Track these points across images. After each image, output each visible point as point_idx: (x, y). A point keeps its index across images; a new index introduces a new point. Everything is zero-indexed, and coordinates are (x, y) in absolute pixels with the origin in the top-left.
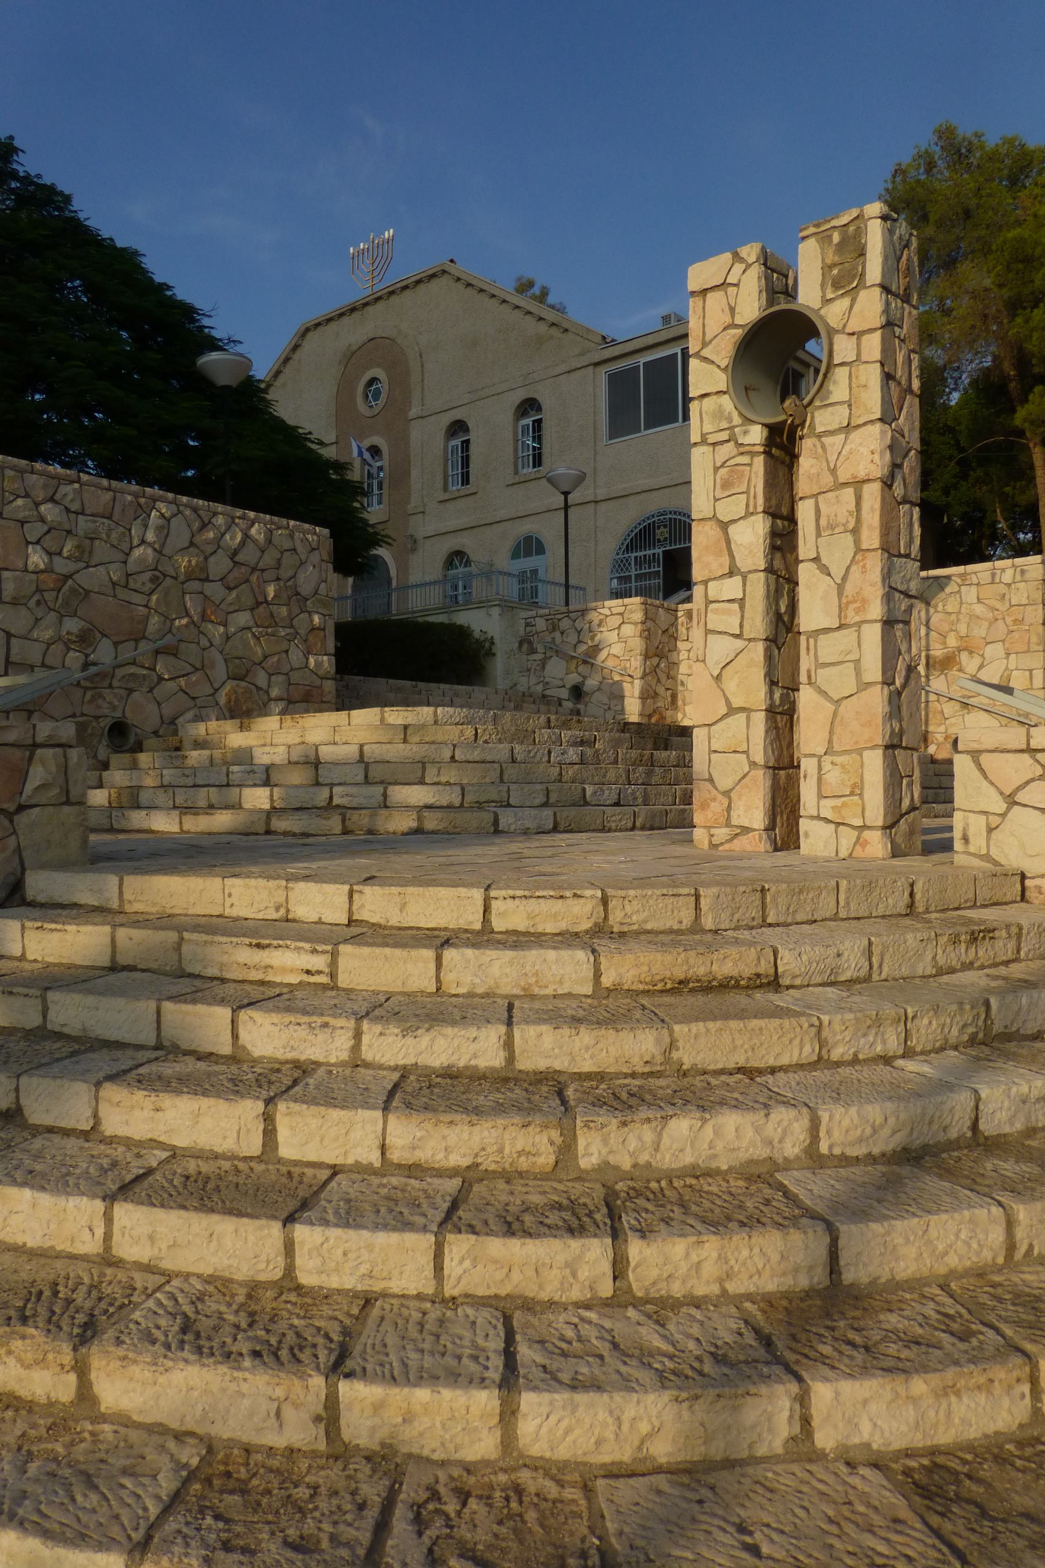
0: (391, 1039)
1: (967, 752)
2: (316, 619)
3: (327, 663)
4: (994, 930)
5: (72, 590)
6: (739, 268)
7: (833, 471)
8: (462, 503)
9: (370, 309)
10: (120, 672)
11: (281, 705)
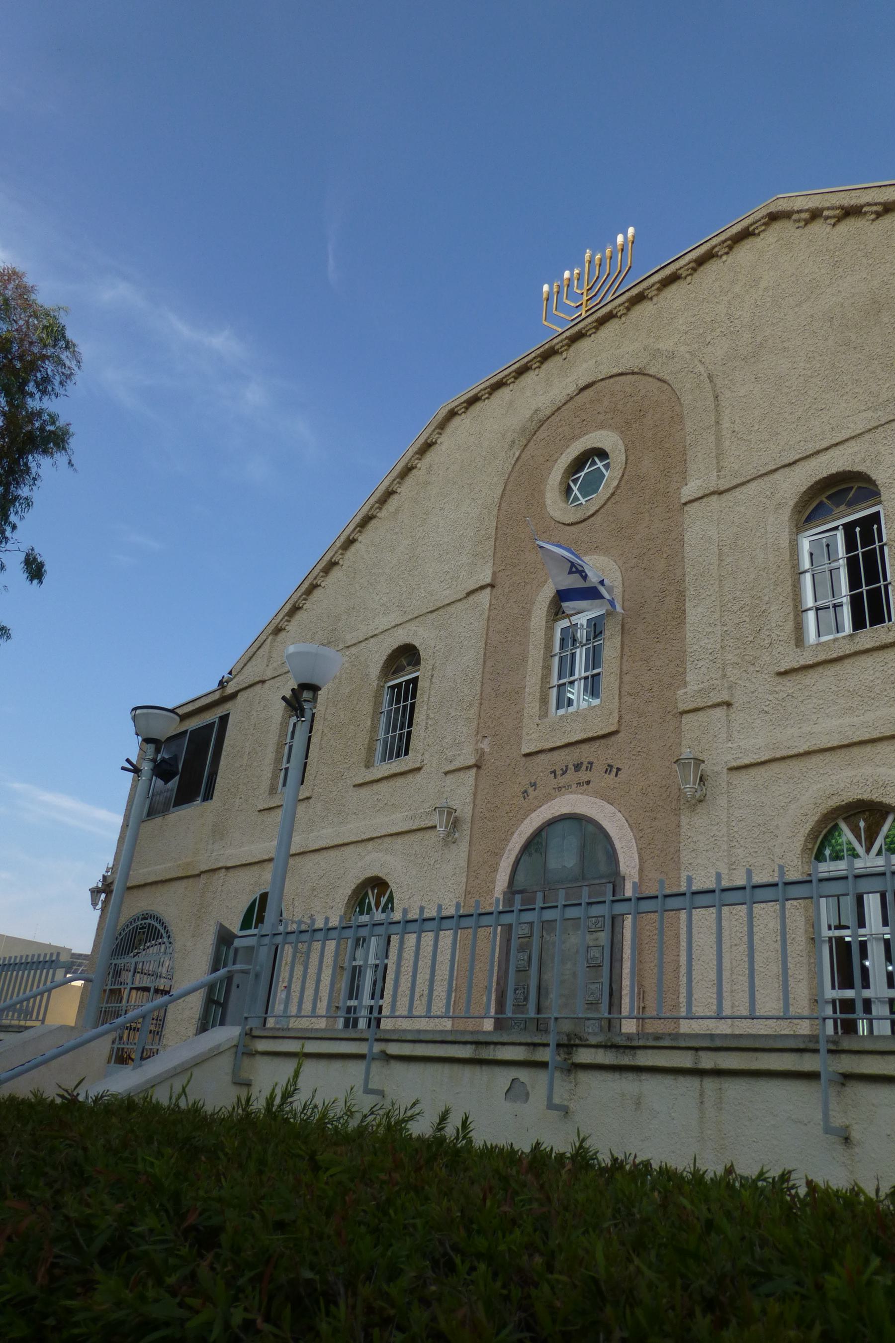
9: (584, 345)
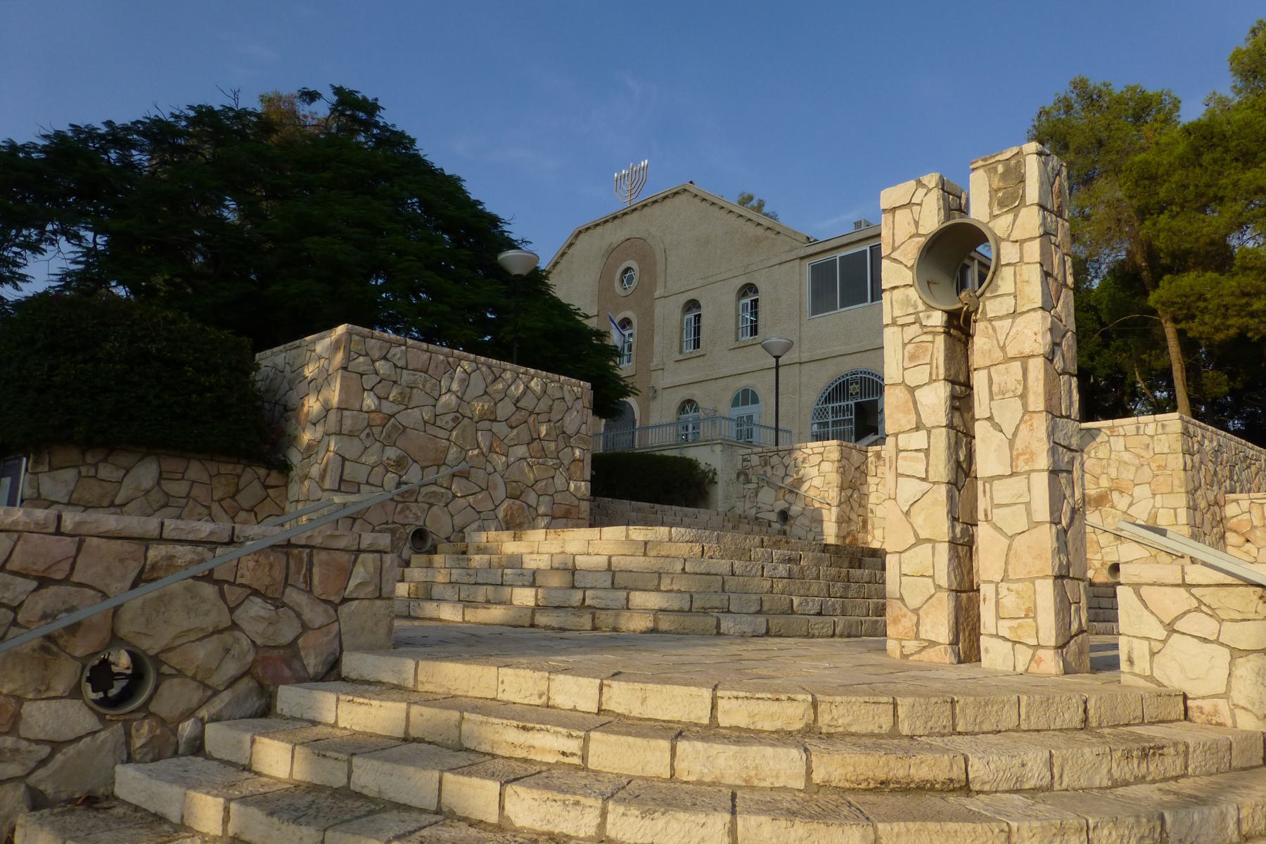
0: (632, 820)
1: (1129, 585)
2: (577, 452)
3: (584, 487)
4: (1163, 747)
5: (394, 426)
6: (921, 192)
7: (1003, 348)
8: (694, 363)
9: (628, 217)
10: (424, 490)
11: (546, 520)
